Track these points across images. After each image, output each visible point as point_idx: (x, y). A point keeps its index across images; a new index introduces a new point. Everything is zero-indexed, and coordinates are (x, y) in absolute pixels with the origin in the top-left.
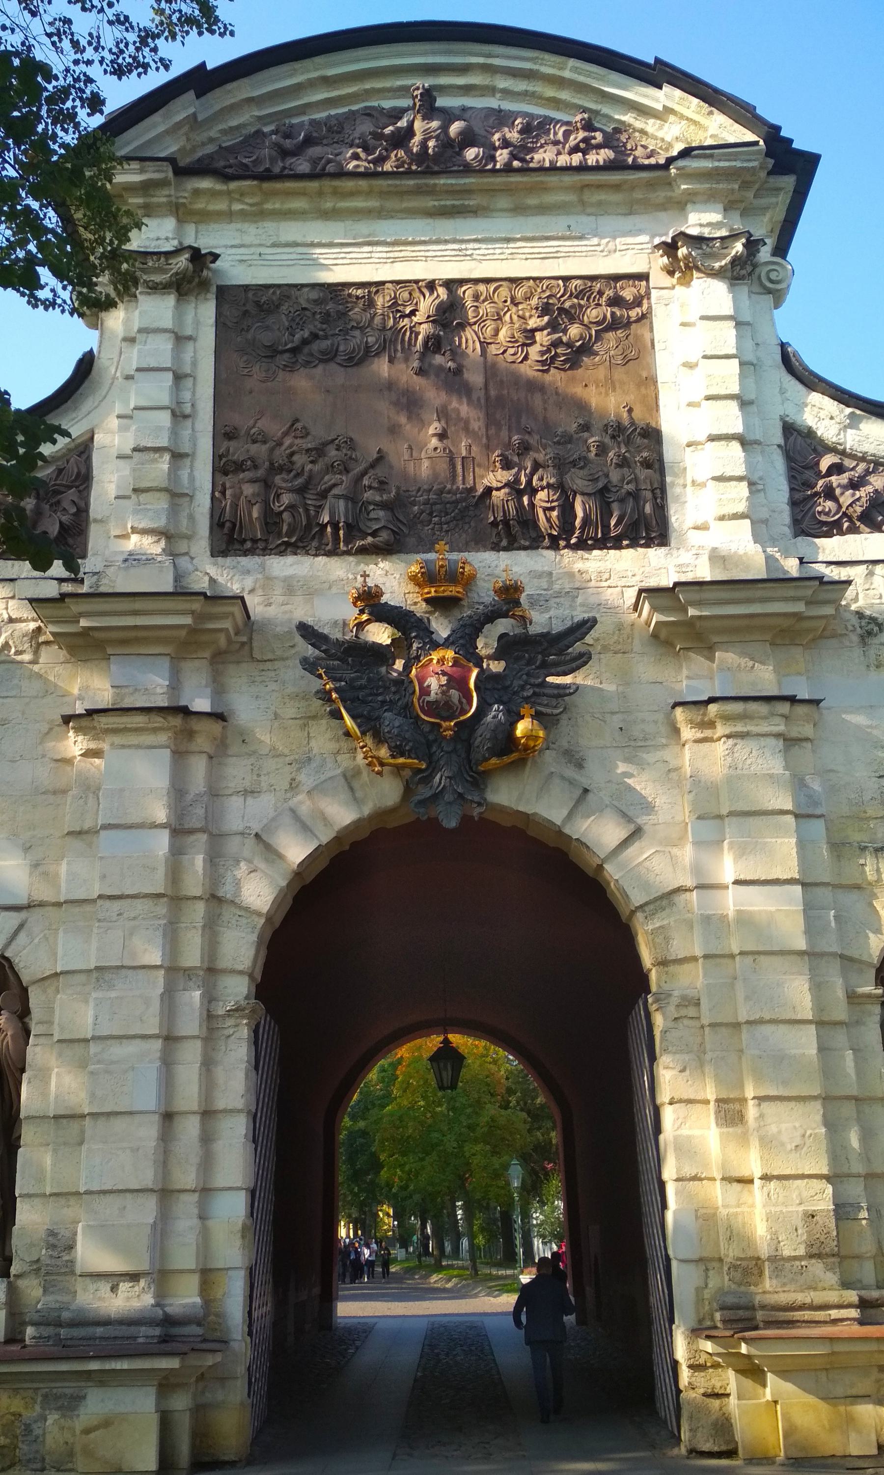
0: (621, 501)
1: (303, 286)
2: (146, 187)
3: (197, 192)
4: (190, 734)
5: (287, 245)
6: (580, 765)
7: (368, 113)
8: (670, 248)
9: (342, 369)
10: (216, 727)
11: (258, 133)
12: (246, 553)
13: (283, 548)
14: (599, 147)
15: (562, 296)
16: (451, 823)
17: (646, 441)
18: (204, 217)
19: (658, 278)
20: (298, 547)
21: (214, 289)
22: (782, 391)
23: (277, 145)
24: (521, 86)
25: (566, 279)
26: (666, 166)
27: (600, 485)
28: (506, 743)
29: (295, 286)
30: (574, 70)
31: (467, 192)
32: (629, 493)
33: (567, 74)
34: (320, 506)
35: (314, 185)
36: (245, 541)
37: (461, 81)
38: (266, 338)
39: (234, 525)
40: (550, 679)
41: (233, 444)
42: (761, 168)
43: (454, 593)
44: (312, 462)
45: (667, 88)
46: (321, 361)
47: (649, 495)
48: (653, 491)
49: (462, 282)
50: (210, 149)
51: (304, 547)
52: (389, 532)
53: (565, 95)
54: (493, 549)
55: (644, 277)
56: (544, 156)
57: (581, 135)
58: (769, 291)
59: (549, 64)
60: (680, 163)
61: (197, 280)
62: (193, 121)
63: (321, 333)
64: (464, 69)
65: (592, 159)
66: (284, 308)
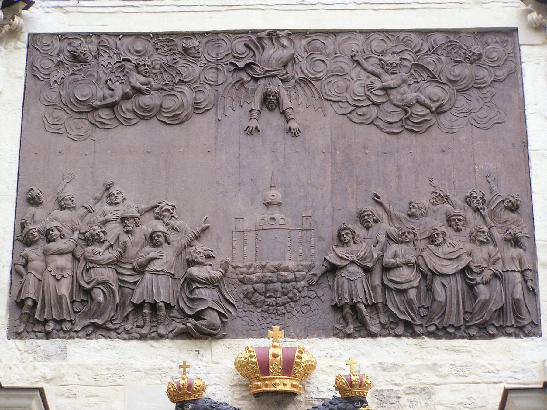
0: (486, 283)
1: (126, 35)
9: (168, 127)
12: (48, 335)
13: (90, 330)
15: (418, 51)
17: (515, 215)
20: (109, 330)
21: (25, 37)
27: (462, 264)
29: (116, 35)
32: (495, 275)
34: (136, 283)
36: (46, 322)
38: (83, 92)
39: (35, 303)
41: (39, 212)
43: (288, 388)
44: (128, 232)
46: (142, 118)
47: (518, 276)
48: (523, 273)
51: (115, 330)
52: (215, 314)
54: (336, 335)
55: (512, 32)
61: (7, 27)
63: (144, 87)
66: (105, 59)
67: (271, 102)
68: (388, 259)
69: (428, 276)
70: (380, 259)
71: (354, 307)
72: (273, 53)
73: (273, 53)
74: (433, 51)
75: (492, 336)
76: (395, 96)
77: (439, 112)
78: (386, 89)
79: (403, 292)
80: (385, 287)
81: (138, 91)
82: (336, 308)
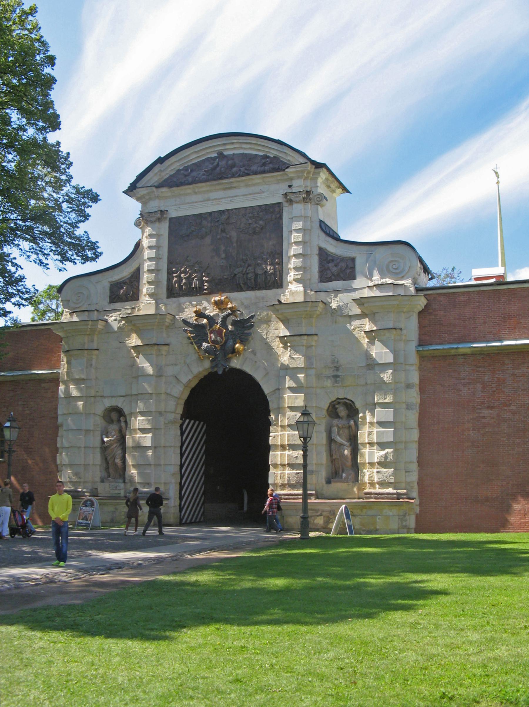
2: (148, 193)
3: (162, 192)
4: (159, 350)
5: (186, 204)
6: (255, 354)
7: (207, 159)
8: (286, 195)
10: (166, 348)
11: (179, 170)
12: (175, 297)
14: (269, 164)
16: (220, 372)
18: (166, 198)
19: (285, 204)
21: (168, 219)
22: (319, 236)
23: (183, 174)
24: (248, 146)
25: (260, 206)
26: (284, 170)
28: (234, 351)
30: (261, 142)
31: (232, 182)
33: (259, 143)
35: (191, 186)
37: (232, 146)
40: (246, 331)
42: (311, 168)
45: (284, 147)
49: (232, 209)
50: (168, 176)
53: (260, 148)
56: (254, 168)
57: (263, 161)
58: (318, 204)
59: (253, 140)
60: (286, 170)
62: (161, 171)
64: (233, 143)
65: (267, 168)
67: (223, 231)
68: (248, 272)
69: (256, 275)
70: (246, 271)
71: (239, 284)
72: (224, 217)
73: (224, 217)
74: (261, 211)
75: (271, 289)
76: (251, 226)
77: (262, 229)
78: (249, 224)
79: (250, 280)
80: (247, 279)
81: (193, 231)
82: (236, 284)
